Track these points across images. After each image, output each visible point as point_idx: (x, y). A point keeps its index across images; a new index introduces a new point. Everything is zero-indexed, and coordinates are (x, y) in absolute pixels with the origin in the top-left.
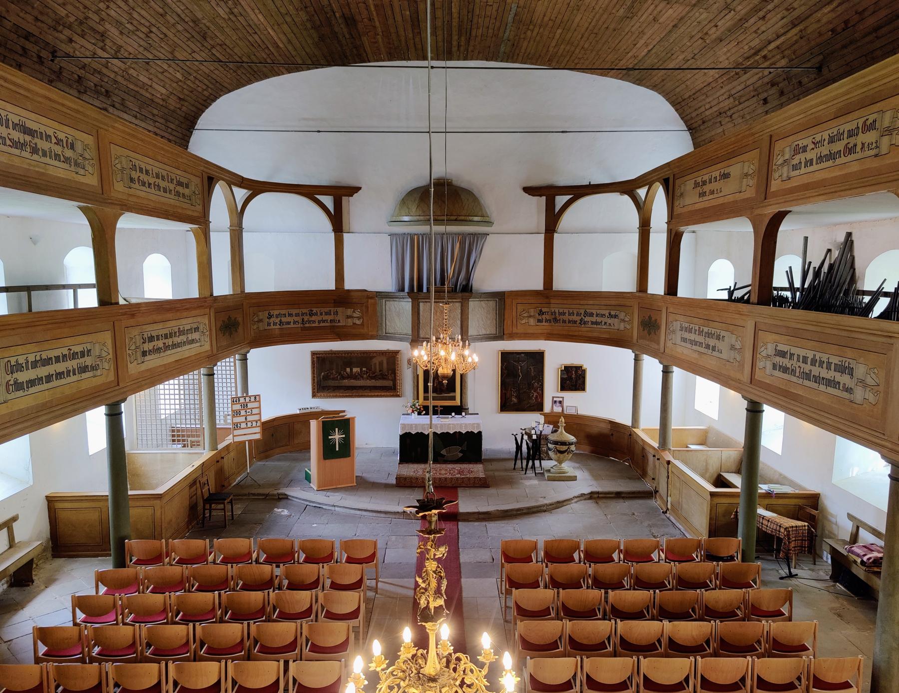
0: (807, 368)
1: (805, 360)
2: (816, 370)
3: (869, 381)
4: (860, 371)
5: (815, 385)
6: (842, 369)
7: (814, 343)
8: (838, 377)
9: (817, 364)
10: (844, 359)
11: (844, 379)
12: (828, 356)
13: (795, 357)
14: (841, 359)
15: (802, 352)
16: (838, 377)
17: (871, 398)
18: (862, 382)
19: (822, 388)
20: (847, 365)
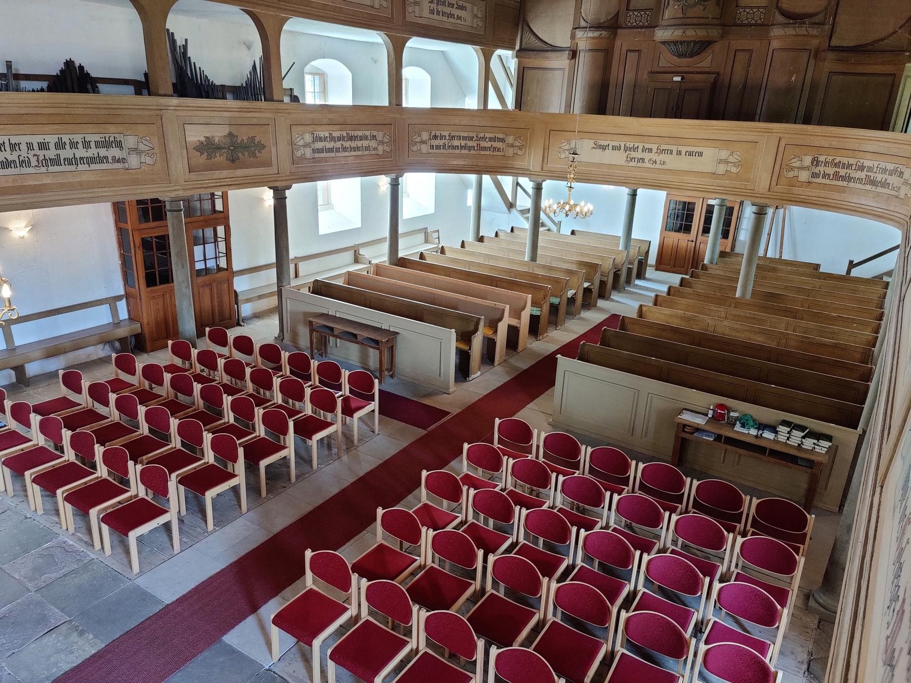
0: (51, 153)
1: (43, 146)
2: (67, 153)
3: (142, 147)
4: (130, 141)
5: (73, 168)
6: (106, 144)
7: (56, 127)
8: (103, 152)
9: (68, 147)
10: (107, 136)
11: (115, 152)
12: (82, 136)
13: (24, 147)
14: (103, 135)
15: (36, 140)
16: (103, 152)
17: (149, 160)
18: (136, 150)
19: (81, 167)
20: (112, 139)
